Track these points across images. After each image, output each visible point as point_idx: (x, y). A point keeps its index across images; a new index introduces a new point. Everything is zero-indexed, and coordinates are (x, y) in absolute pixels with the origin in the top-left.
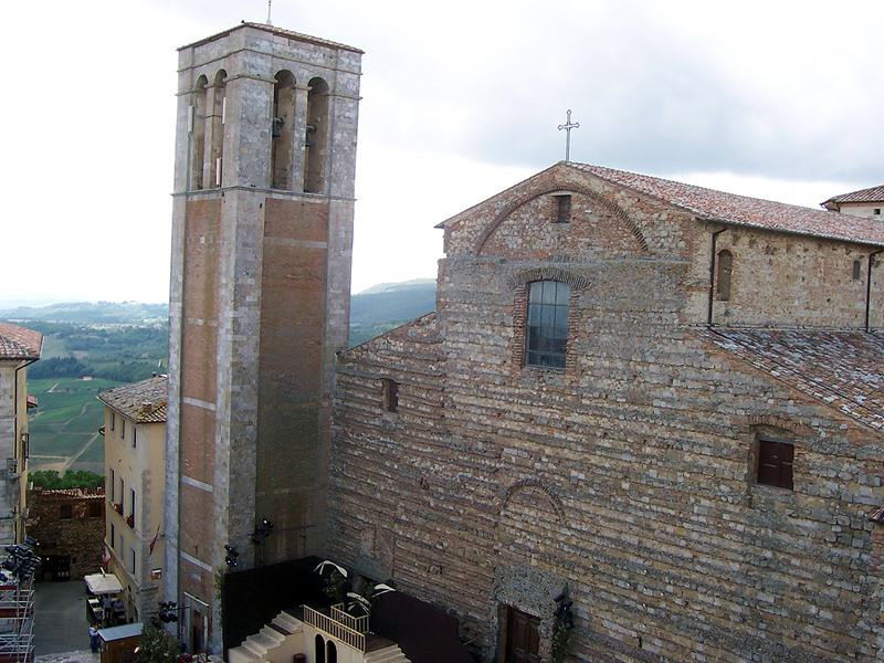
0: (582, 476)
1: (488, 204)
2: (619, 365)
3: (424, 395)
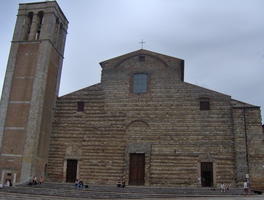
0: (154, 116)
2: (163, 90)
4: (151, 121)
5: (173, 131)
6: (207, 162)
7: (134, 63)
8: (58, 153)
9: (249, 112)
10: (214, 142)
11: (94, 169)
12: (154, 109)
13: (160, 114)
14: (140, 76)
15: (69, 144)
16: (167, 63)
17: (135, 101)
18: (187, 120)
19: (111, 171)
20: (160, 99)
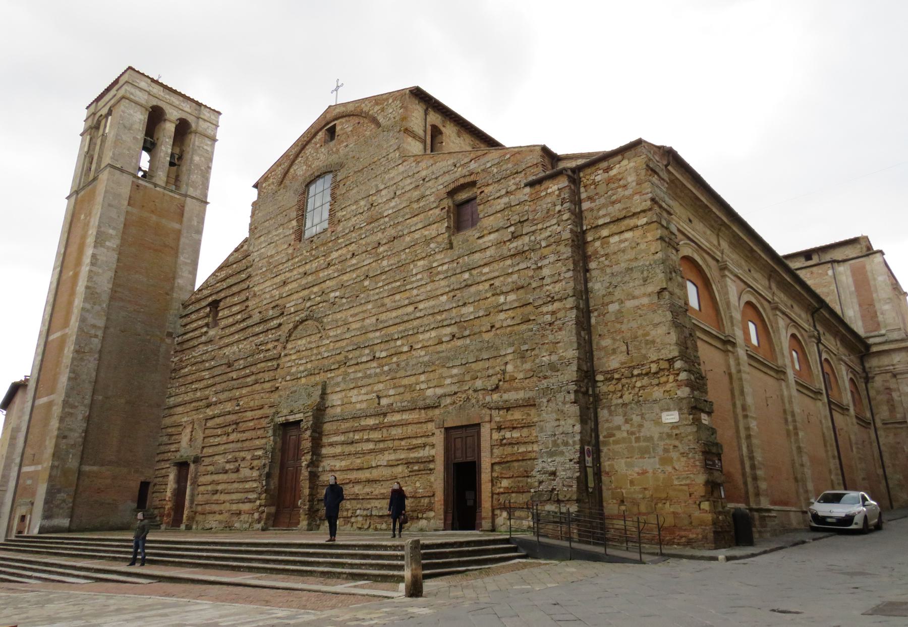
0: (337, 294)
1: (286, 155)
2: (362, 203)
9: (598, 178)
10: (488, 342)
18: (414, 279)
19: (247, 486)
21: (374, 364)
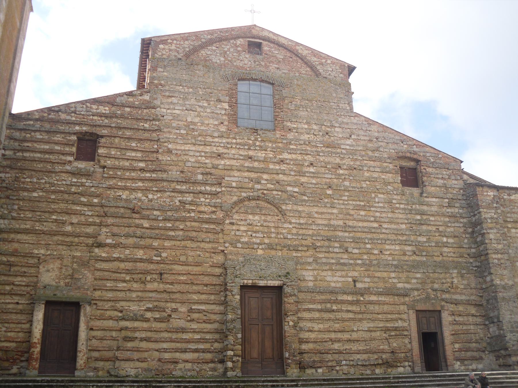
0: (296, 190)
1: (196, 35)
2: (315, 127)
3: (134, 145)
4: (291, 203)
5: (346, 231)
6: (429, 311)
7: (235, 54)
8: (11, 279)
9: (505, 197)
10: (440, 263)
11: (135, 330)
12: (295, 171)
13: (311, 186)
14: (255, 87)
15: (49, 252)
16: (318, 68)
17: (246, 147)
18: (377, 205)
19: (185, 336)
20: (308, 148)
21: (345, 256)
